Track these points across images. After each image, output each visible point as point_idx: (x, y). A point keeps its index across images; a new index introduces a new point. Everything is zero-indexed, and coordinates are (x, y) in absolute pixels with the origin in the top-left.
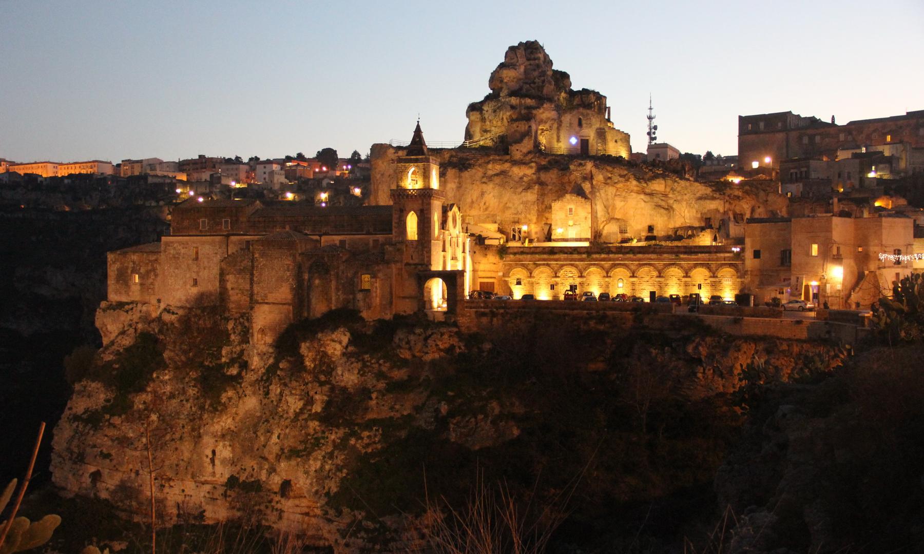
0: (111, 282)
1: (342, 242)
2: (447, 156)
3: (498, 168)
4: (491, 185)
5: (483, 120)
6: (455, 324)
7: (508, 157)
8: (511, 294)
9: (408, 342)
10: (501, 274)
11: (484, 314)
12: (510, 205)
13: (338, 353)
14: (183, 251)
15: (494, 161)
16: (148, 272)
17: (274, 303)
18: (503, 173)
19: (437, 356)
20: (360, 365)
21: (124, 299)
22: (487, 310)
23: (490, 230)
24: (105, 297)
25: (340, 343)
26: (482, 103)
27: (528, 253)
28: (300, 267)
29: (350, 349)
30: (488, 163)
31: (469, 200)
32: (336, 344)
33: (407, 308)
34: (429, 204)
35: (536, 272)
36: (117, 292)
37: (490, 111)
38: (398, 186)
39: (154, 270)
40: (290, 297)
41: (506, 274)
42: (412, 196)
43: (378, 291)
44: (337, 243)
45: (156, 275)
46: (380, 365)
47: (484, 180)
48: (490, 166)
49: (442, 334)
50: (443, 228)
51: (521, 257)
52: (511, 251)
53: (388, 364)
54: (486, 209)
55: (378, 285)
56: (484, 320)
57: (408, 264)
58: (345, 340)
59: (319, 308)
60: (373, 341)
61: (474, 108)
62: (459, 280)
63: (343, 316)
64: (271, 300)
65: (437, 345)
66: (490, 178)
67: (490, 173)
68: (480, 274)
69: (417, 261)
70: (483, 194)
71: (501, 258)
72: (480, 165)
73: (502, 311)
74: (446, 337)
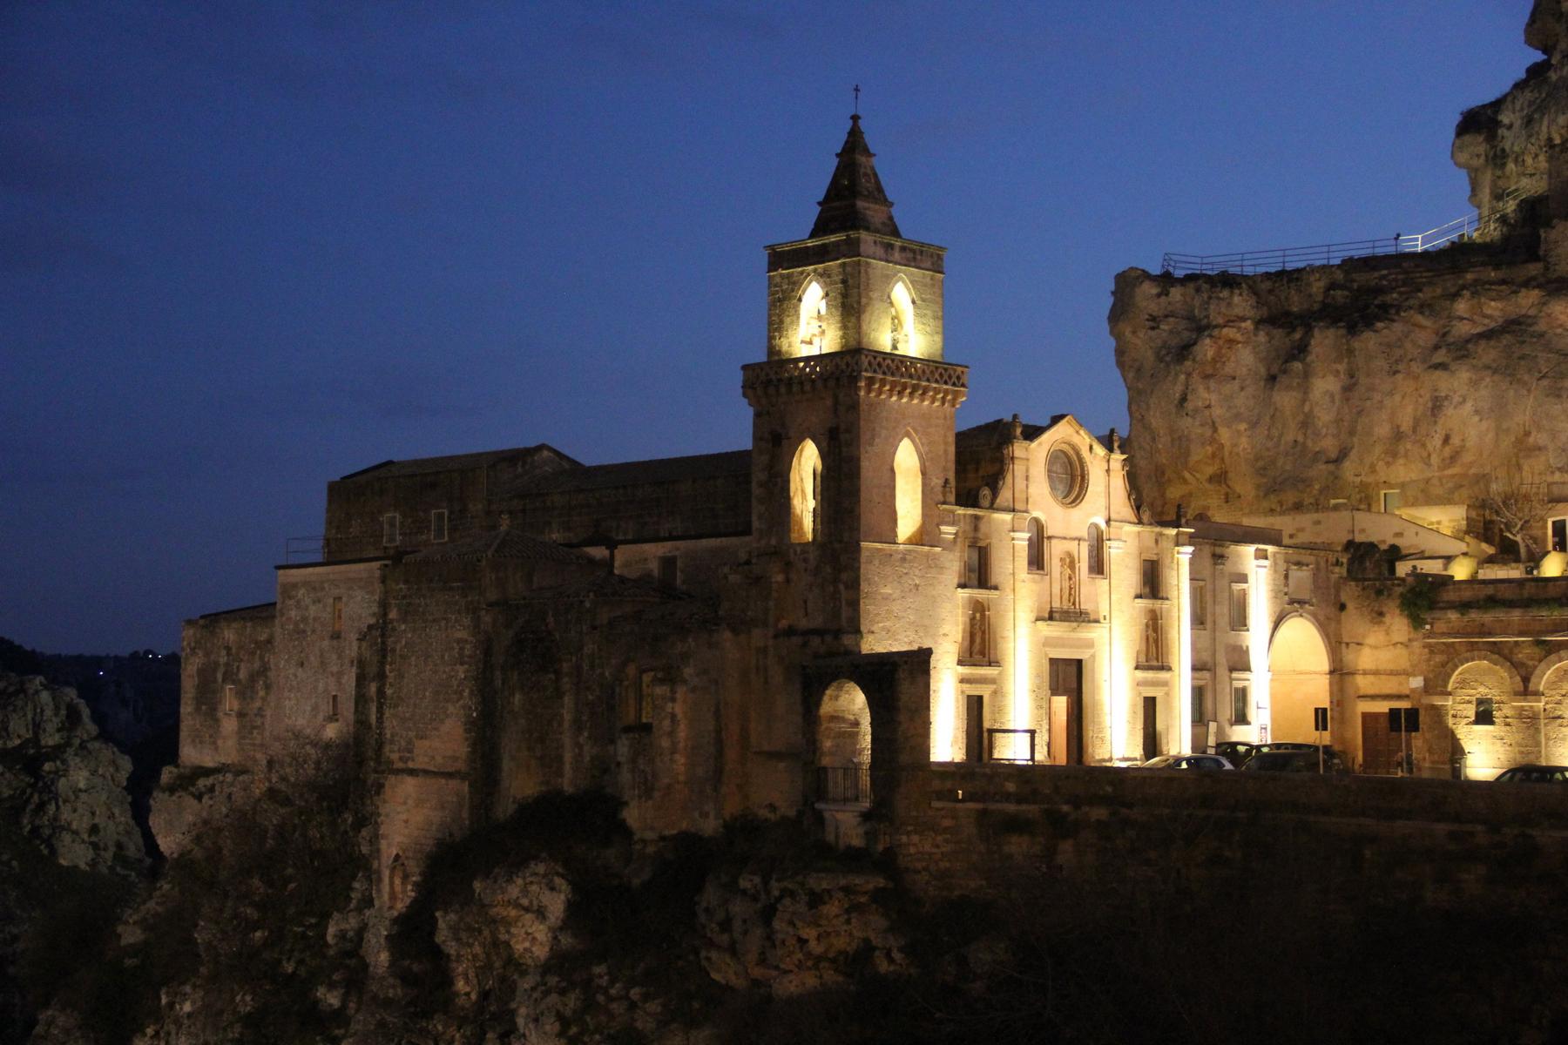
0: (186, 708)
1: (668, 563)
2: (1317, 286)
3: (1495, 309)
4: (1464, 375)
5: (1498, 158)
6: (887, 863)
7: (1534, 269)
8: (1456, 752)
9: (726, 925)
10: (1417, 682)
11: (1015, 825)
12: (1538, 438)
13: (541, 952)
14: (313, 610)
15: (1477, 288)
16: (253, 678)
17: (426, 772)
18: (1515, 326)
19: (811, 981)
20: (572, 1001)
21: (209, 761)
22: (1031, 810)
23: (1437, 533)
24: (172, 756)
25: (541, 913)
26: (1497, 105)
27: (1510, 604)
28: (488, 652)
29: (566, 941)
30: (1455, 296)
31: (1383, 430)
32: (532, 917)
33: (774, 792)
34: (854, 407)
35: (1546, 676)
36: (197, 739)
37: (1518, 123)
38: (773, 351)
39: (264, 670)
40: (463, 750)
41: (1436, 684)
42: (803, 380)
43: (682, 733)
44: (654, 566)
45: (268, 687)
46: (633, 1006)
47: (1441, 356)
48: (1461, 307)
49: (816, 900)
50: (967, 498)
51: (1488, 617)
52: (1450, 595)
53: (654, 1006)
54: (1453, 458)
55: (678, 709)
56: (1017, 846)
57: (791, 632)
58: (557, 904)
59: (520, 784)
60: (642, 910)
61: (1478, 122)
62: (906, 690)
63: (570, 826)
64: (420, 762)
65: (803, 942)
66: (1462, 350)
67: (1463, 329)
68: (1364, 683)
69: (817, 621)
70: (1437, 406)
71: (1416, 622)
72: (1421, 309)
73: (1099, 813)
74: (831, 909)
